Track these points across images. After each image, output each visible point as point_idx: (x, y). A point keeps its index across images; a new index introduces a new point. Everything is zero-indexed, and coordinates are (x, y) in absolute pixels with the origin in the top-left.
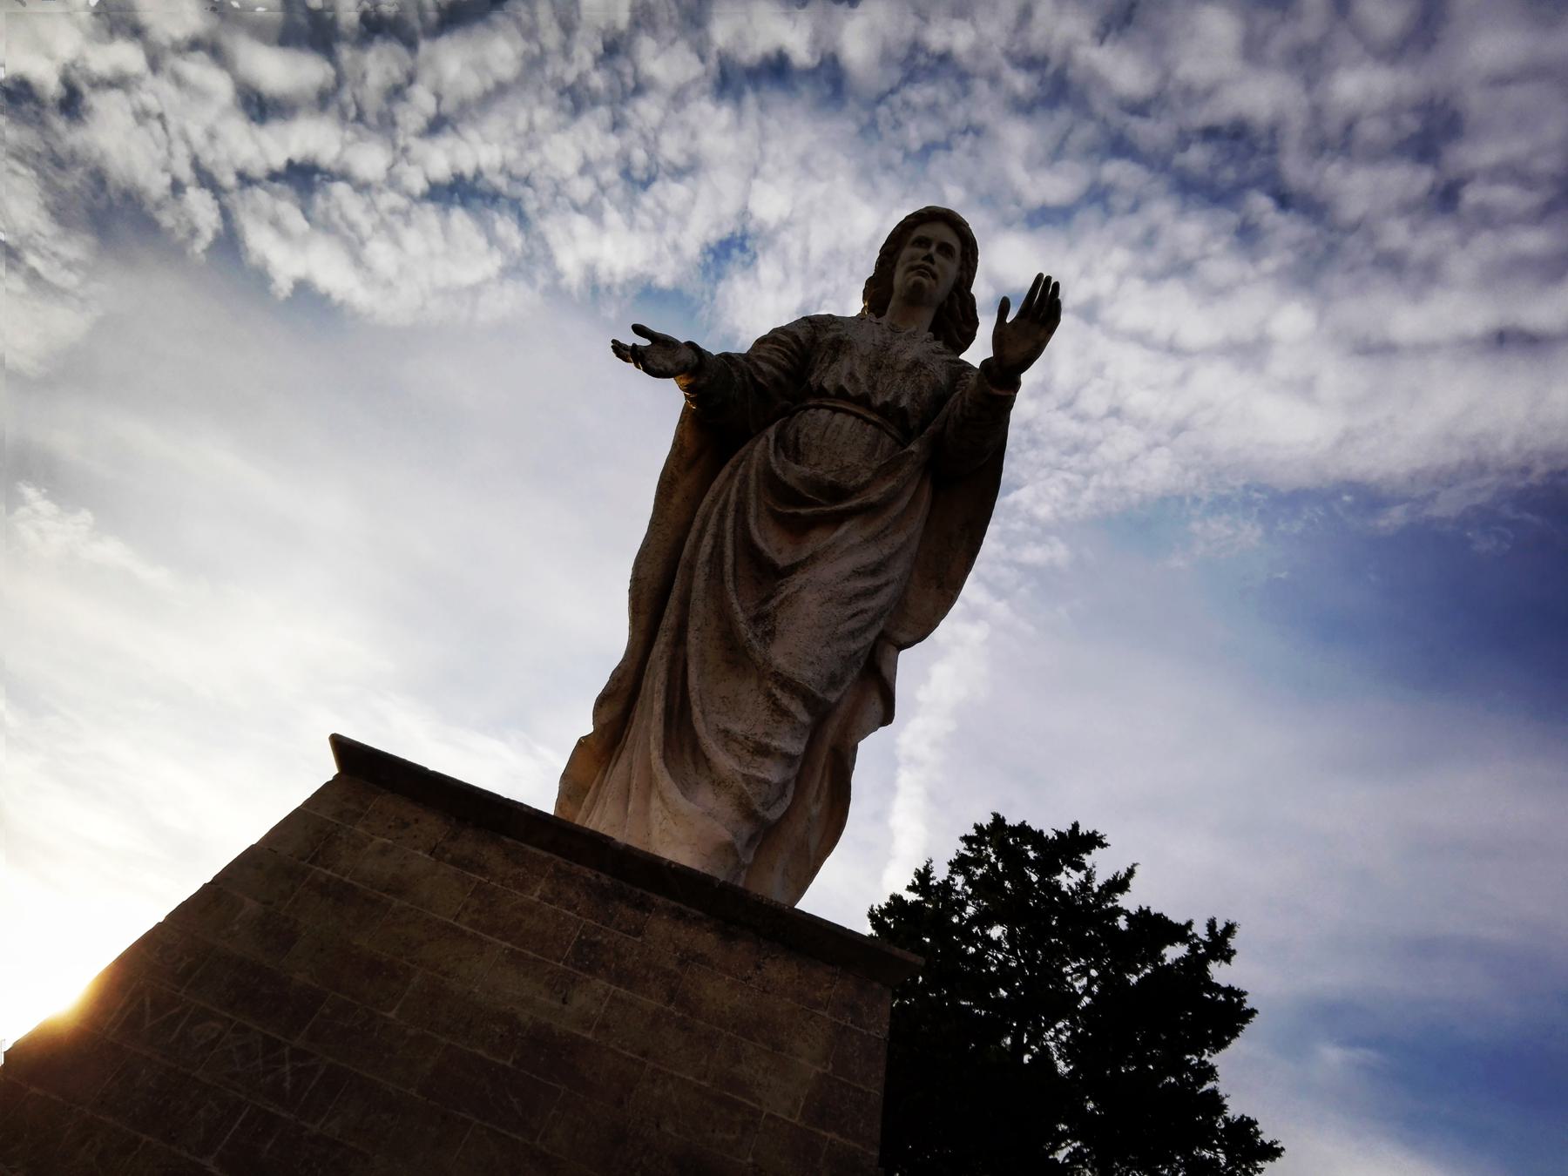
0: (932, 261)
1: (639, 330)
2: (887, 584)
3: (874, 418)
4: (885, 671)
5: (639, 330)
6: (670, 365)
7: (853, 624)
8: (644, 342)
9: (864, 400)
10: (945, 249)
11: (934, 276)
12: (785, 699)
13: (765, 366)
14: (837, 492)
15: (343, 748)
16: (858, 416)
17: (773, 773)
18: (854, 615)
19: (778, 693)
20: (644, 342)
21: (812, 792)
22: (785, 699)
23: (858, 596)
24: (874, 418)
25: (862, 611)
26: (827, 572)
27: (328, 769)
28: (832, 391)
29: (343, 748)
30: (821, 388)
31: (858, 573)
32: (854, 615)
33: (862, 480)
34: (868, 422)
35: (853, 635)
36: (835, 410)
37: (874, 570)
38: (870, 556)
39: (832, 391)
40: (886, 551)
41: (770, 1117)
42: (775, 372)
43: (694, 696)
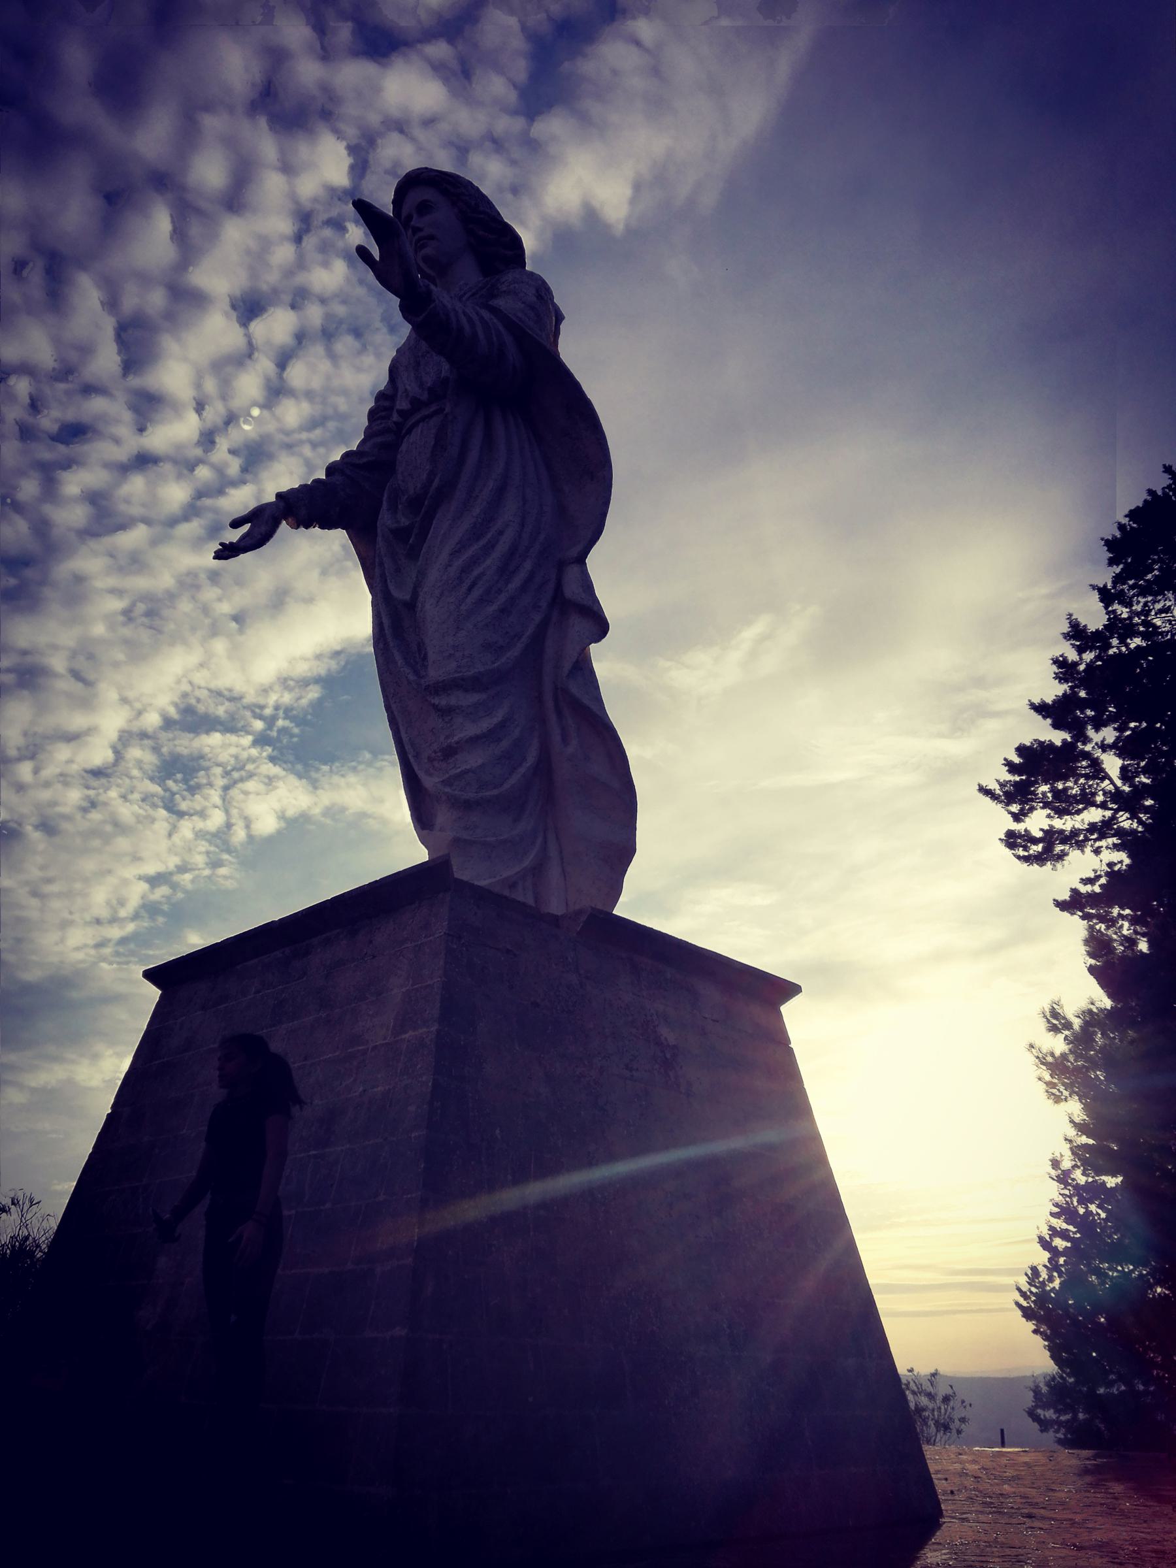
0: (420, 230)
1: (236, 524)
2: (501, 533)
3: (433, 408)
4: (571, 590)
5: (236, 524)
6: (263, 529)
7: (477, 593)
8: (246, 528)
9: (417, 405)
10: (424, 208)
11: (431, 237)
12: (442, 701)
13: (367, 448)
14: (415, 504)
15: (150, 975)
16: (423, 419)
17: (473, 760)
18: (470, 589)
19: (436, 701)
20: (246, 528)
21: (556, 737)
22: (442, 701)
23: (465, 570)
24: (433, 408)
25: (483, 574)
26: (433, 575)
27: (154, 993)
28: (401, 420)
29: (150, 975)
30: (395, 423)
31: (455, 553)
32: (470, 589)
33: (424, 476)
34: (430, 416)
35: (482, 601)
36: (409, 431)
37: (476, 533)
38: (466, 524)
39: (401, 420)
40: (477, 511)
41: (375, 1047)
42: (379, 439)
43: (407, 747)
